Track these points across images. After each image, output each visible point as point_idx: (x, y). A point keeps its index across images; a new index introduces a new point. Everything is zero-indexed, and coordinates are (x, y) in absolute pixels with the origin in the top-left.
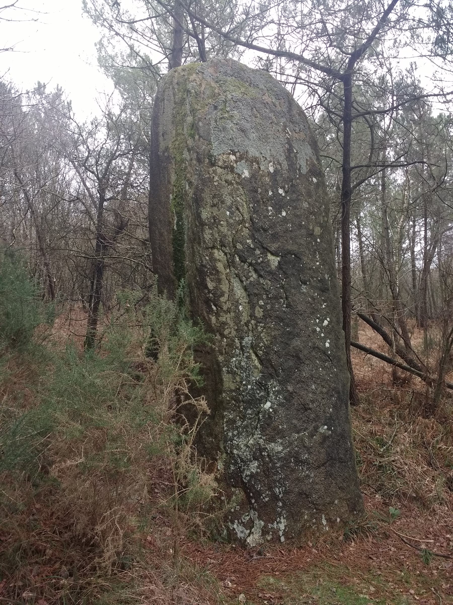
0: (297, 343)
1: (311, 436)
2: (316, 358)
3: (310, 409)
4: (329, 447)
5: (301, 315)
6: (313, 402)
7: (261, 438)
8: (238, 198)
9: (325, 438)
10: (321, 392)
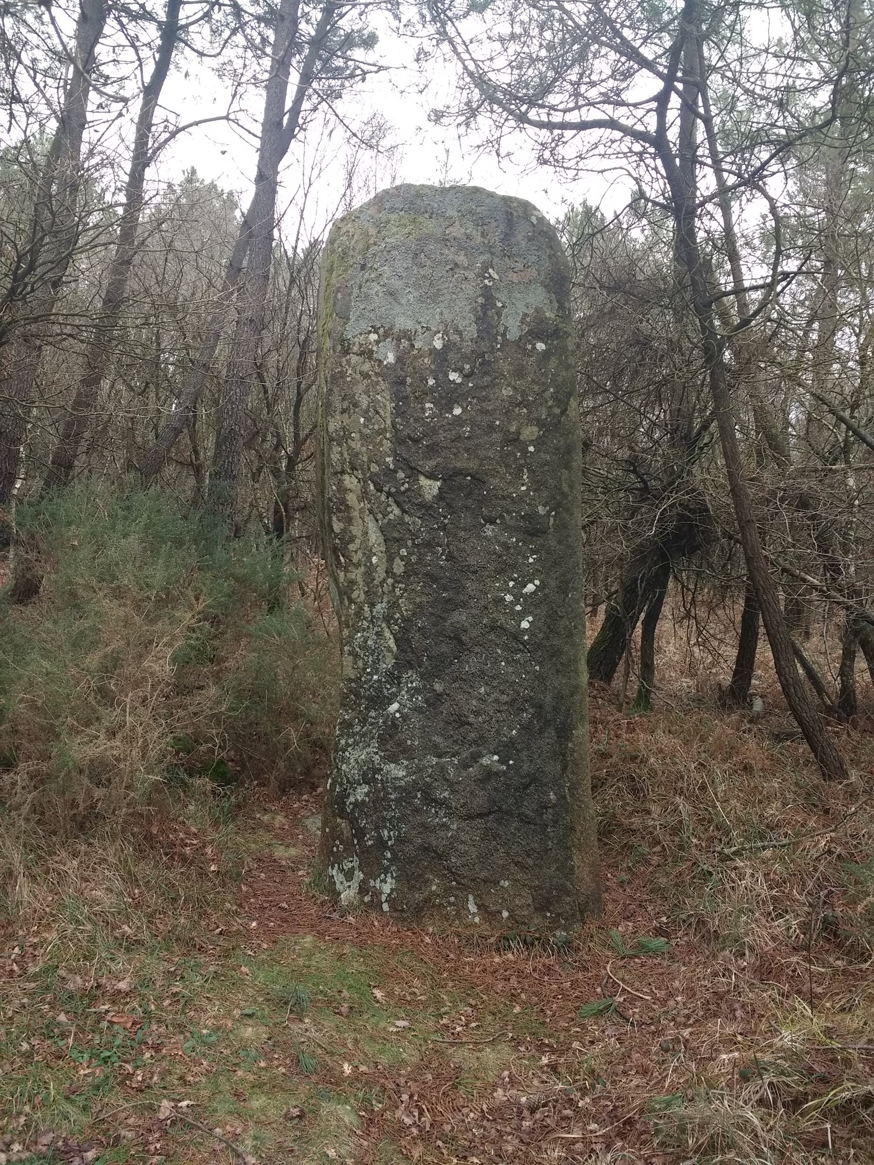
0: (460, 617)
1: (465, 766)
2: (497, 645)
3: (469, 724)
4: (496, 789)
5: (475, 572)
6: (477, 713)
7: (376, 753)
9: (489, 774)
10: (497, 701)
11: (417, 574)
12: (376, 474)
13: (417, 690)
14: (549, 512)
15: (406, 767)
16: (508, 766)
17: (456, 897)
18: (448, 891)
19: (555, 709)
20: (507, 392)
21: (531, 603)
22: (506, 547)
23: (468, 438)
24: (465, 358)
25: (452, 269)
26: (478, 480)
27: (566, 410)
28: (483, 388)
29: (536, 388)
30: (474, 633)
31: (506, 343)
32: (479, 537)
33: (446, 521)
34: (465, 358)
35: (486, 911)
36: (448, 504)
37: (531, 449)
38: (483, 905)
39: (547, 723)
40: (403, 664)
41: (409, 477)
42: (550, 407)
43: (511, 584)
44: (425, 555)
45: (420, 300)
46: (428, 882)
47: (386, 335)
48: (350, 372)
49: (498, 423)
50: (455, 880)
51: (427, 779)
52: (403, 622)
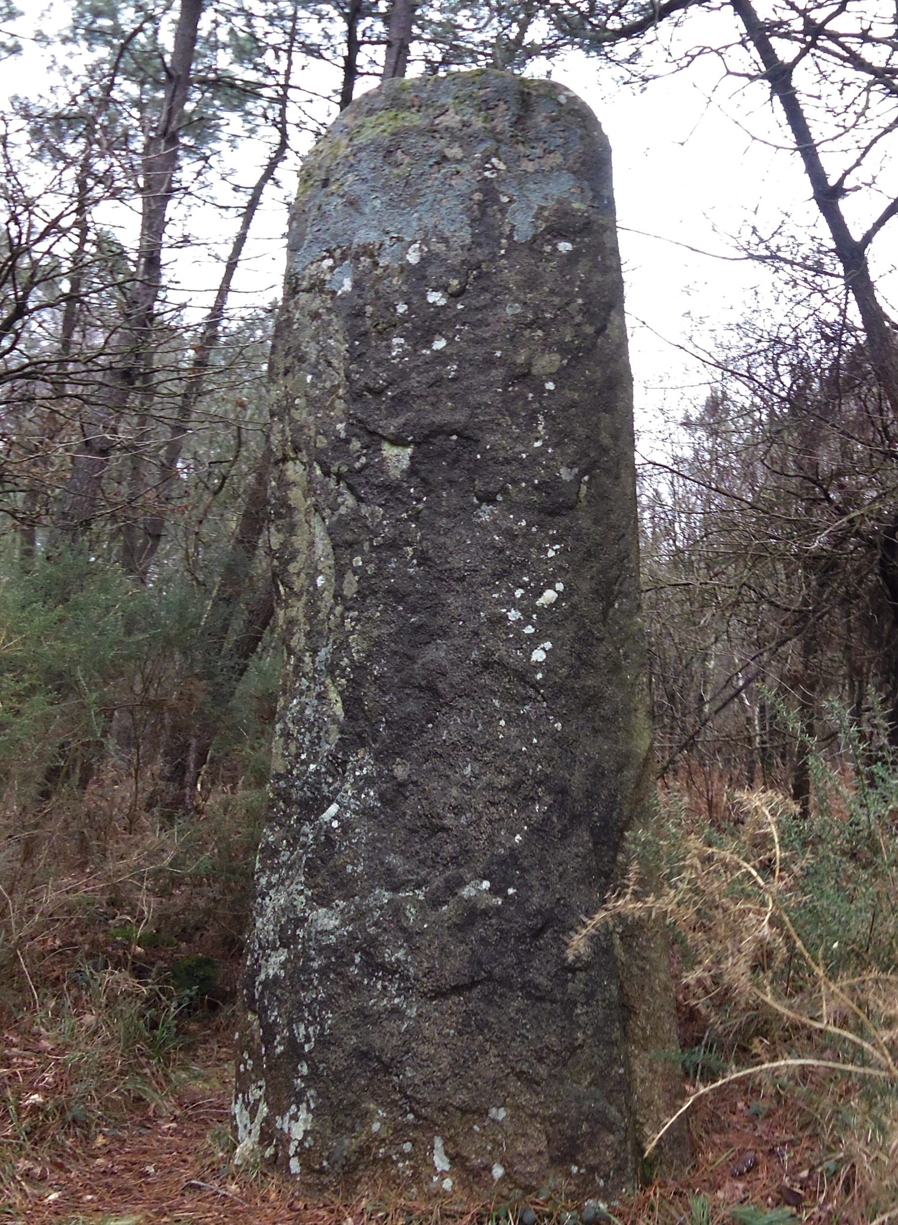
0: (437, 653)
1: (435, 902)
3: (444, 829)
4: (483, 941)
5: (462, 579)
6: (458, 810)
7: (301, 892)
8: (332, 342)
9: (473, 914)
10: (490, 786)
11: (374, 593)
12: (323, 451)
13: (369, 781)
14: (578, 480)
15: (342, 911)
16: (506, 897)
17: (414, 1142)
18: (399, 1131)
19: (590, 795)
20: (512, 310)
21: (549, 622)
22: (510, 535)
23: (454, 380)
24: (452, 271)
25: (437, 163)
26: (468, 438)
27: (604, 328)
28: (478, 309)
29: (556, 300)
30: (457, 676)
31: (513, 247)
32: (471, 526)
33: (420, 506)
34: (452, 271)
35: (464, 1168)
36: (423, 480)
37: (550, 386)
38: (458, 1155)
39: (575, 819)
40: (352, 740)
41: (367, 447)
42: (578, 325)
43: (519, 593)
44: (387, 561)
45: (391, 204)
46: (365, 1116)
47: (344, 257)
48: (297, 316)
49: (498, 354)
50: (412, 1111)
51: (372, 930)
52: (353, 671)
